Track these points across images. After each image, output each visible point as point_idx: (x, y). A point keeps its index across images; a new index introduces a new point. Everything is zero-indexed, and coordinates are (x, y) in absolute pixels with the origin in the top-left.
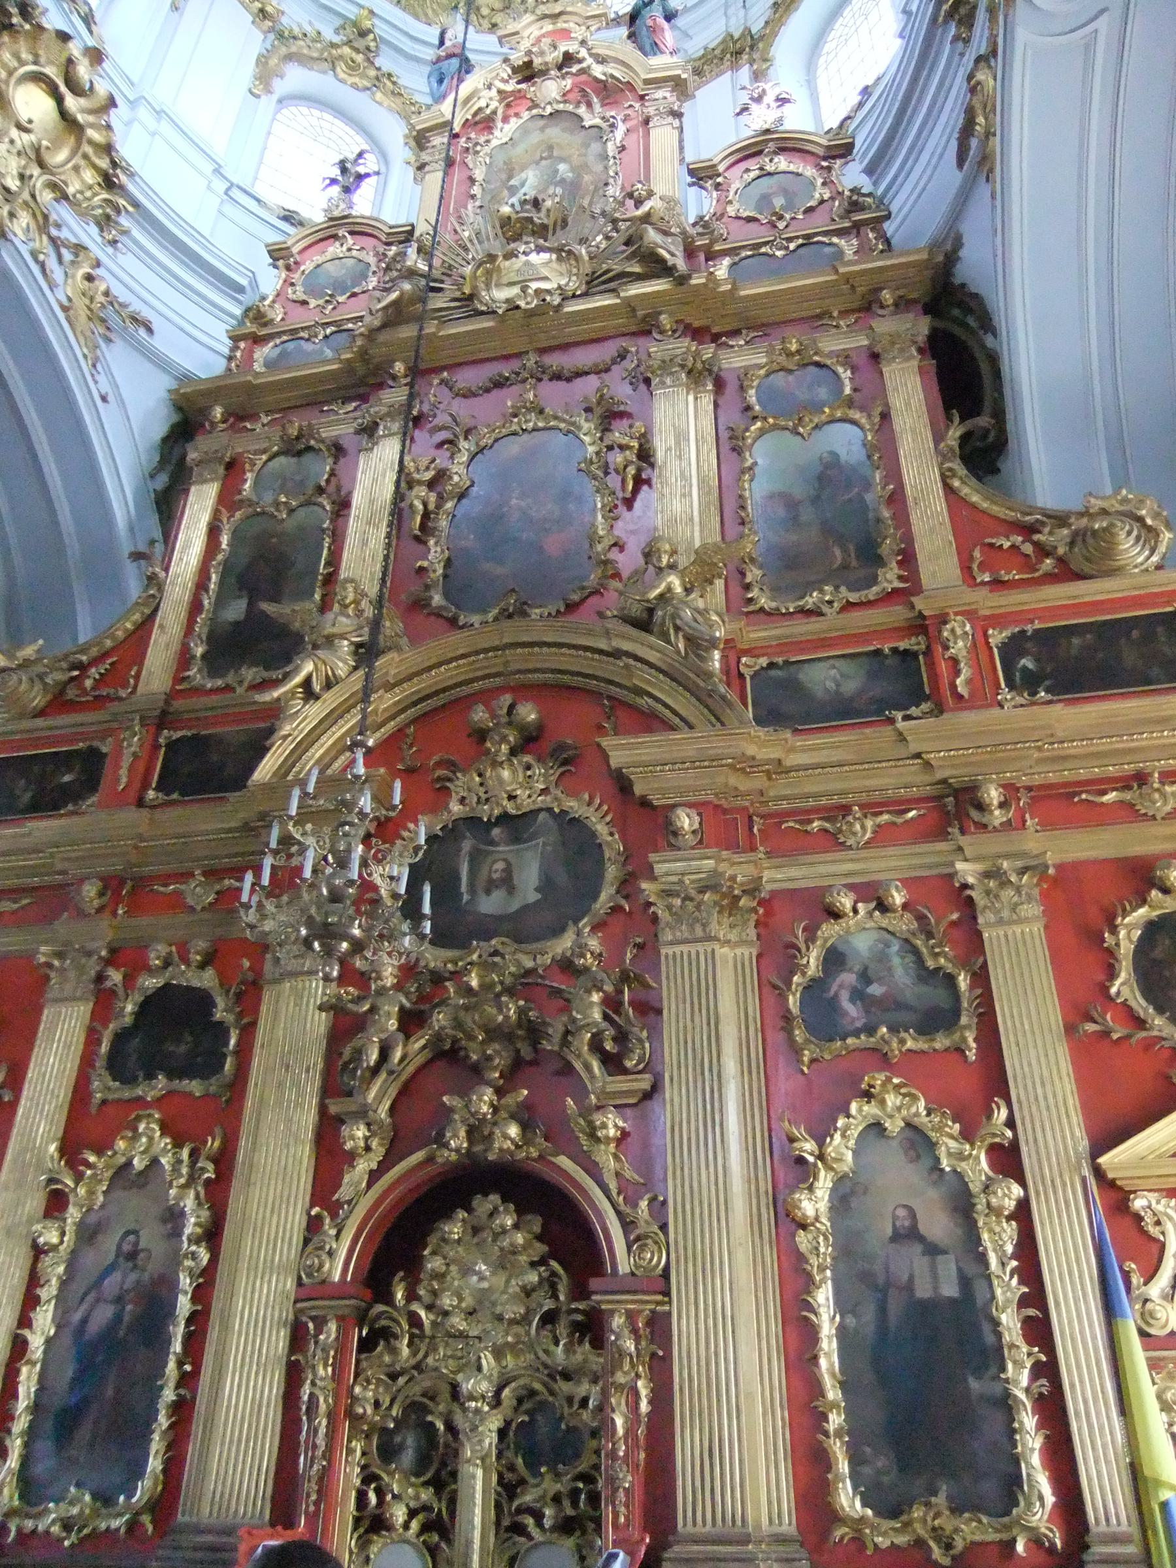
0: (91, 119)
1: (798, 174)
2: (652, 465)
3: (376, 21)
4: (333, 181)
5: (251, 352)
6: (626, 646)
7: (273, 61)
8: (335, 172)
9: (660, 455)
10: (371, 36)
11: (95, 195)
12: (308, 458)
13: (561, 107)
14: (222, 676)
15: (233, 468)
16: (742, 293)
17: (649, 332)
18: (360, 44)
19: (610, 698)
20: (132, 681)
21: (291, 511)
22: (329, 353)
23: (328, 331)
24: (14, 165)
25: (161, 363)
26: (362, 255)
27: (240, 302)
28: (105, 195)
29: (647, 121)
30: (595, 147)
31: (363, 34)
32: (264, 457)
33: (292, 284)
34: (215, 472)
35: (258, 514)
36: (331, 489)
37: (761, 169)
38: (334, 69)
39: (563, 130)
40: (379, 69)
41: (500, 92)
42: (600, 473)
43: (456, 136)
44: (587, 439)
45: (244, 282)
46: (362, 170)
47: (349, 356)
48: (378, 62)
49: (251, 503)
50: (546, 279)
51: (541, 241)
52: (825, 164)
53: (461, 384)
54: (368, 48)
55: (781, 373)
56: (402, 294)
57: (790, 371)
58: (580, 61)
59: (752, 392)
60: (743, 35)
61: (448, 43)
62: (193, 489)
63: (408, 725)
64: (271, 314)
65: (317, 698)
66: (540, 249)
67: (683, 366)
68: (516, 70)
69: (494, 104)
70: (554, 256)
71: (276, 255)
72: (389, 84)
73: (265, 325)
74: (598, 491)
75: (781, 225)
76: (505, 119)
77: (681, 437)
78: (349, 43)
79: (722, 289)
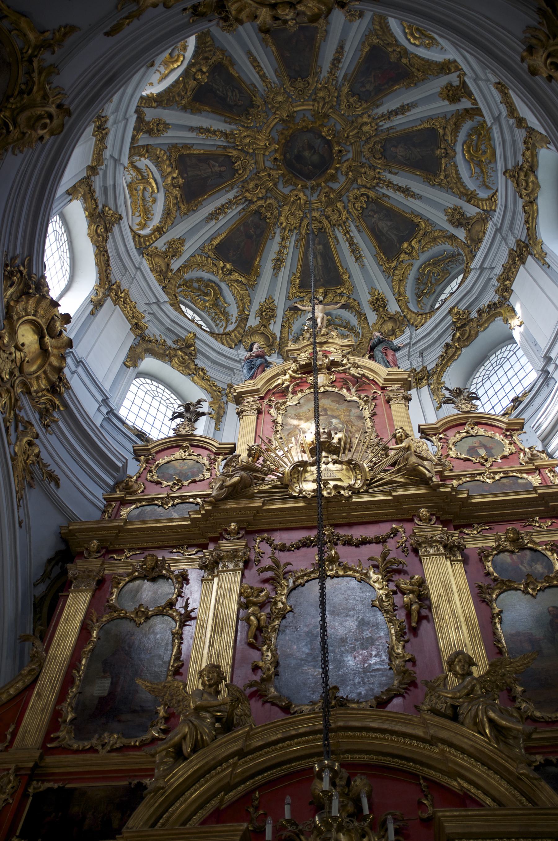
0: (55, 351)
1: (491, 437)
2: (430, 608)
3: (197, 341)
4: (180, 415)
5: (119, 510)
6: (443, 734)
7: (139, 350)
8: (182, 409)
9: (434, 598)
10: (193, 348)
11: (44, 396)
12: (161, 582)
13: (330, 389)
14: (89, 739)
15: (101, 584)
16: (473, 501)
17: (412, 520)
18: (188, 351)
19: (425, 779)
20: (9, 737)
21: (148, 618)
22: (175, 515)
23: (176, 501)
24: (8, 366)
25: (59, 507)
26: (200, 459)
27: (115, 478)
28: (49, 396)
29: (388, 401)
30: (355, 411)
31: (189, 346)
32: (127, 579)
33: (151, 471)
34: (89, 585)
35: (122, 618)
36: (179, 606)
37: (467, 432)
38: (171, 361)
39: (333, 401)
40: (196, 365)
41: (291, 376)
42: (390, 608)
43: (262, 398)
44: (377, 585)
45: (120, 465)
46: (201, 410)
47: (197, 516)
48: (197, 361)
49: (113, 608)
50: (340, 480)
51: (335, 457)
52: (508, 433)
53: (276, 542)
54: (191, 354)
55: (506, 554)
56: (241, 477)
57: (512, 552)
58: (343, 365)
59: (489, 564)
60: (422, 370)
61: (254, 350)
62: (71, 595)
63: (253, 791)
64: (136, 487)
65: (185, 759)
66: (335, 462)
67: (441, 543)
68: (302, 367)
69: (287, 383)
70: (344, 467)
71: (139, 453)
72: (201, 373)
73: (130, 493)
74: (390, 621)
75: (488, 465)
76: (294, 393)
77: (447, 588)
78: (180, 349)
79: (461, 496)
